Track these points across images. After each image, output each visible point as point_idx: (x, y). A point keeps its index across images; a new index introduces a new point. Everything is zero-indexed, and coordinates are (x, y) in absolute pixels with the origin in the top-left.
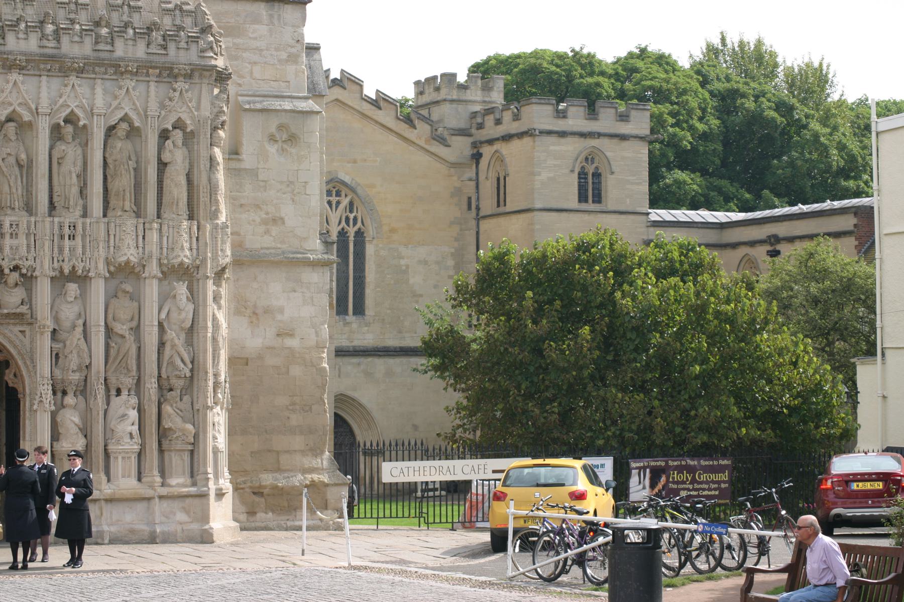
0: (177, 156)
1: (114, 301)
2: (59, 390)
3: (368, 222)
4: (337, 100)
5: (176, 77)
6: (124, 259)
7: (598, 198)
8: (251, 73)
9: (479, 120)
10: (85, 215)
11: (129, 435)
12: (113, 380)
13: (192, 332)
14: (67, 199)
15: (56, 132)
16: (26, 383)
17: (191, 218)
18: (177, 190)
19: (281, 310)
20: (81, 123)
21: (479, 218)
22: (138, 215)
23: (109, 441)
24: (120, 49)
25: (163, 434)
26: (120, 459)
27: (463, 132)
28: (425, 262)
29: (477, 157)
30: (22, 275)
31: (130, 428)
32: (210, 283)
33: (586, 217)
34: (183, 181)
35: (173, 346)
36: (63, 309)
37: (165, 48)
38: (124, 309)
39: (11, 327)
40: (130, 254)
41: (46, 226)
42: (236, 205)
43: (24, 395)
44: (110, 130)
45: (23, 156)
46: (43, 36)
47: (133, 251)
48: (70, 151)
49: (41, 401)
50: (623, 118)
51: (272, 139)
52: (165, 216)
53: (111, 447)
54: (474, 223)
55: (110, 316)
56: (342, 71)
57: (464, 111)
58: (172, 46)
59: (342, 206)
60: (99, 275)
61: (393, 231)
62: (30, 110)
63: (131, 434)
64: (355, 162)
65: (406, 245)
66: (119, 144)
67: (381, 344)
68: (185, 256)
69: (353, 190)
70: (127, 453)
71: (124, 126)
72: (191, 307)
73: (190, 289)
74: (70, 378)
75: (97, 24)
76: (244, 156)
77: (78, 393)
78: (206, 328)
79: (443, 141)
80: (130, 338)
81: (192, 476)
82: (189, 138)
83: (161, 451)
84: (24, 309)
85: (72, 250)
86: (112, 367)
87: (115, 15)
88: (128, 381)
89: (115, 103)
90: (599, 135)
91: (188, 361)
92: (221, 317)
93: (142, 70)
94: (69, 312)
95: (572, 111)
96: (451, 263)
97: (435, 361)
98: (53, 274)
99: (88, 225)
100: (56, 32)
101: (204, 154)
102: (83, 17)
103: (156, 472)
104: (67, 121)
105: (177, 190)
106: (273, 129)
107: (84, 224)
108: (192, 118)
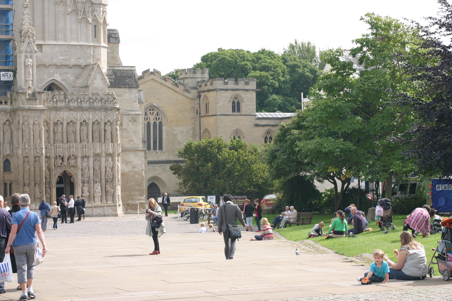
0: (108, 128)
1: (95, 162)
2: (83, 182)
3: (163, 119)
4: (152, 79)
5: (108, 110)
7: (239, 110)
8: (125, 105)
9: (200, 84)
10: (88, 143)
12: (95, 180)
13: (112, 168)
14: (84, 139)
15: (81, 123)
17: (112, 142)
18: (109, 136)
19: (133, 162)
21: (200, 117)
22: (100, 142)
24: (95, 105)
25: (106, 192)
27: (195, 88)
28: (183, 132)
29: (199, 96)
31: (99, 191)
32: (116, 157)
33: (235, 117)
34: (110, 134)
35: (108, 172)
37: (105, 103)
38: (97, 163)
40: (98, 151)
41: (80, 145)
42: (122, 137)
44: (93, 123)
45: (74, 130)
46: (78, 102)
47: (99, 150)
48: (84, 128)
50: (247, 84)
51: (130, 121)
52: (106, 142)
53: (95, 195)
54: (199, 118)
56: (154, 69)
57: (195, 81)
58: (107, 103)
59: (154, 114)
60: (91, 156)
61: (171, 122)
62: (75, 119)
64: (159, 99)
65: (176, 127)
66: (95, 126)
67: (168, 159)
68: (111, 151)
69: (158, 109)
71: (96, 122)
72: (112, 163)
73: (112, 158)
75: (90, 99)
76: (124, 126)
78: (116, 167)
79: (188, 91)
80: (99, 170)
81: (113, 201)
82: (111, 124)
83: (106, 196)
84: (75, 164)
85: (85, 151)
87: (94, 96)
88: (98, 180)
89: (94, 117)
90: (239, 90)
91: (112, 175)
92: (119, 165)
93: (100, 109)
94: (85, 165)
95: (230, 82)
96: (191, 132)
97: (174, 172)
100: (81, 101)
101: (114, 127)
102: (86, 97)
103: (105, 200)
104: (83, 121)
105: (109, 136)
106: (130, 119)
107: (88, 145)
108: (112, 119)
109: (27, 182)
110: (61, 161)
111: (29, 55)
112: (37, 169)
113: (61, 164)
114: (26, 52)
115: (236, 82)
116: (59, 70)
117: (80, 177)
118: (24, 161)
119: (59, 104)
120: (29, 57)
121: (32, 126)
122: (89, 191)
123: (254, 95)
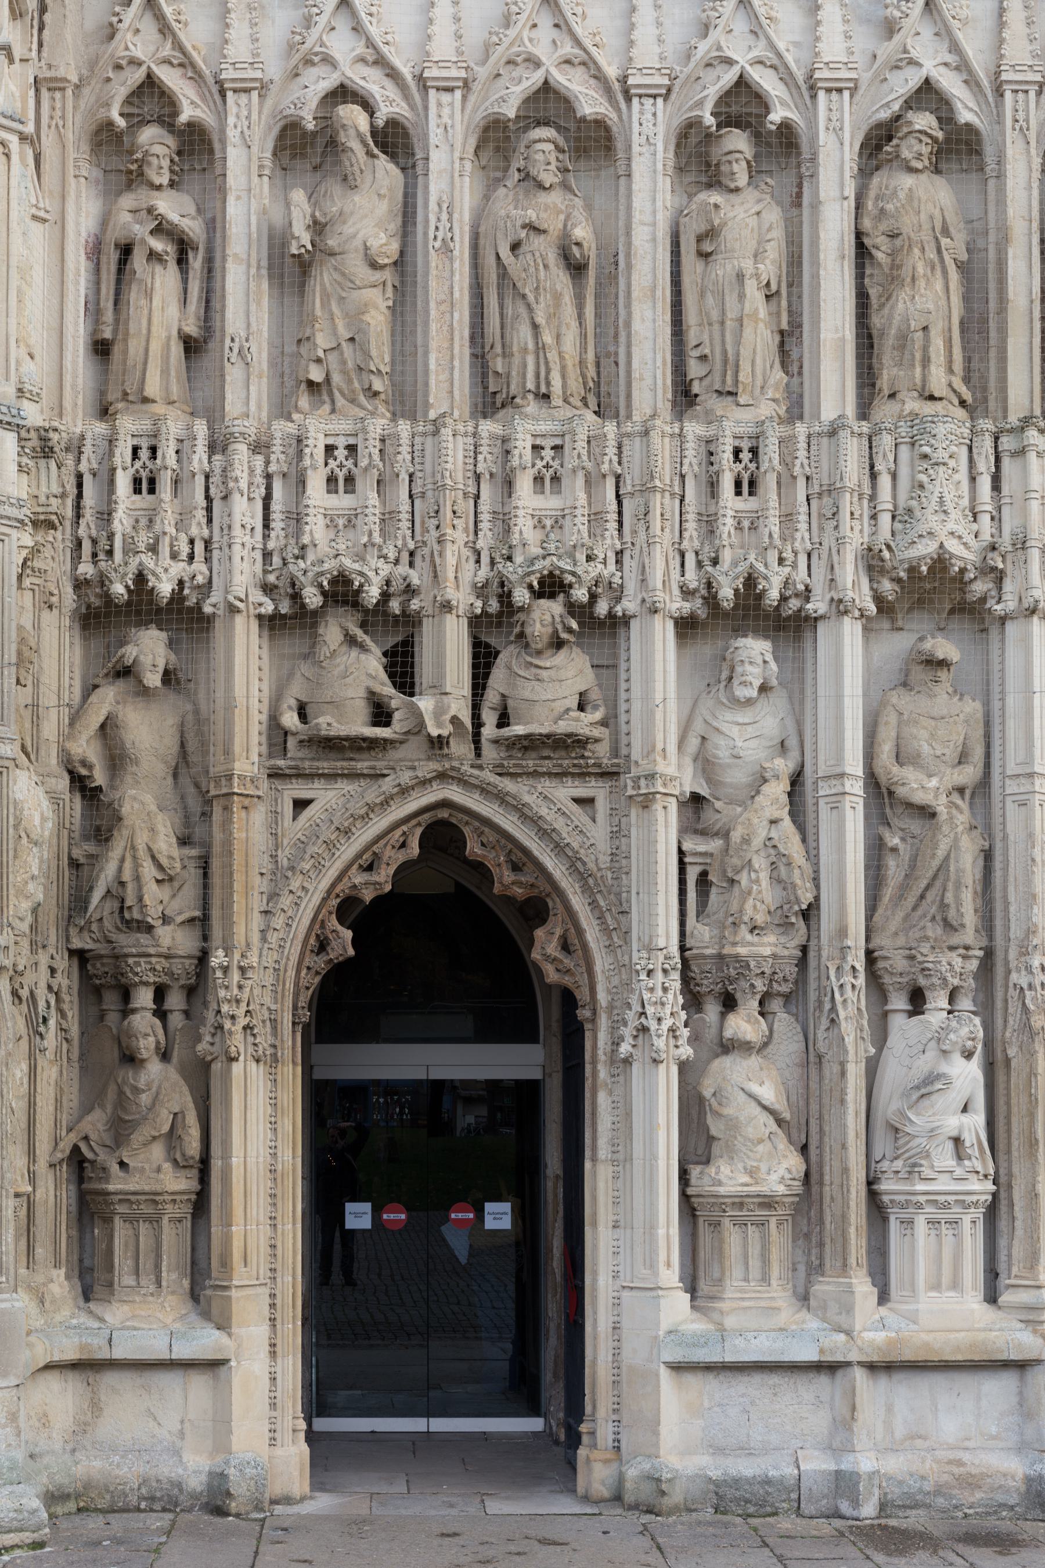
6: (926, 549)
11: (950, 1145)
12: (895, 961)
16: (598, 968)
20: (776, 116)
23: (885, 1165)
26: (920, 1222)
30: (573, 608)
31: (953, 1123)
36: (724, 727)
39: (545, 785)
43: (594, 1012)
45: (581, 232)
47: (957, 522)
49: (645, 1029)
55: (886, 751)
63: (957, 1141)
70: (946, 1206)
74: (742, 951)
77: (776, 1005)
84: (584, 724)
86: (891, 918)
89: (887, 50)
98: (686, 607)
99: (802, 445)
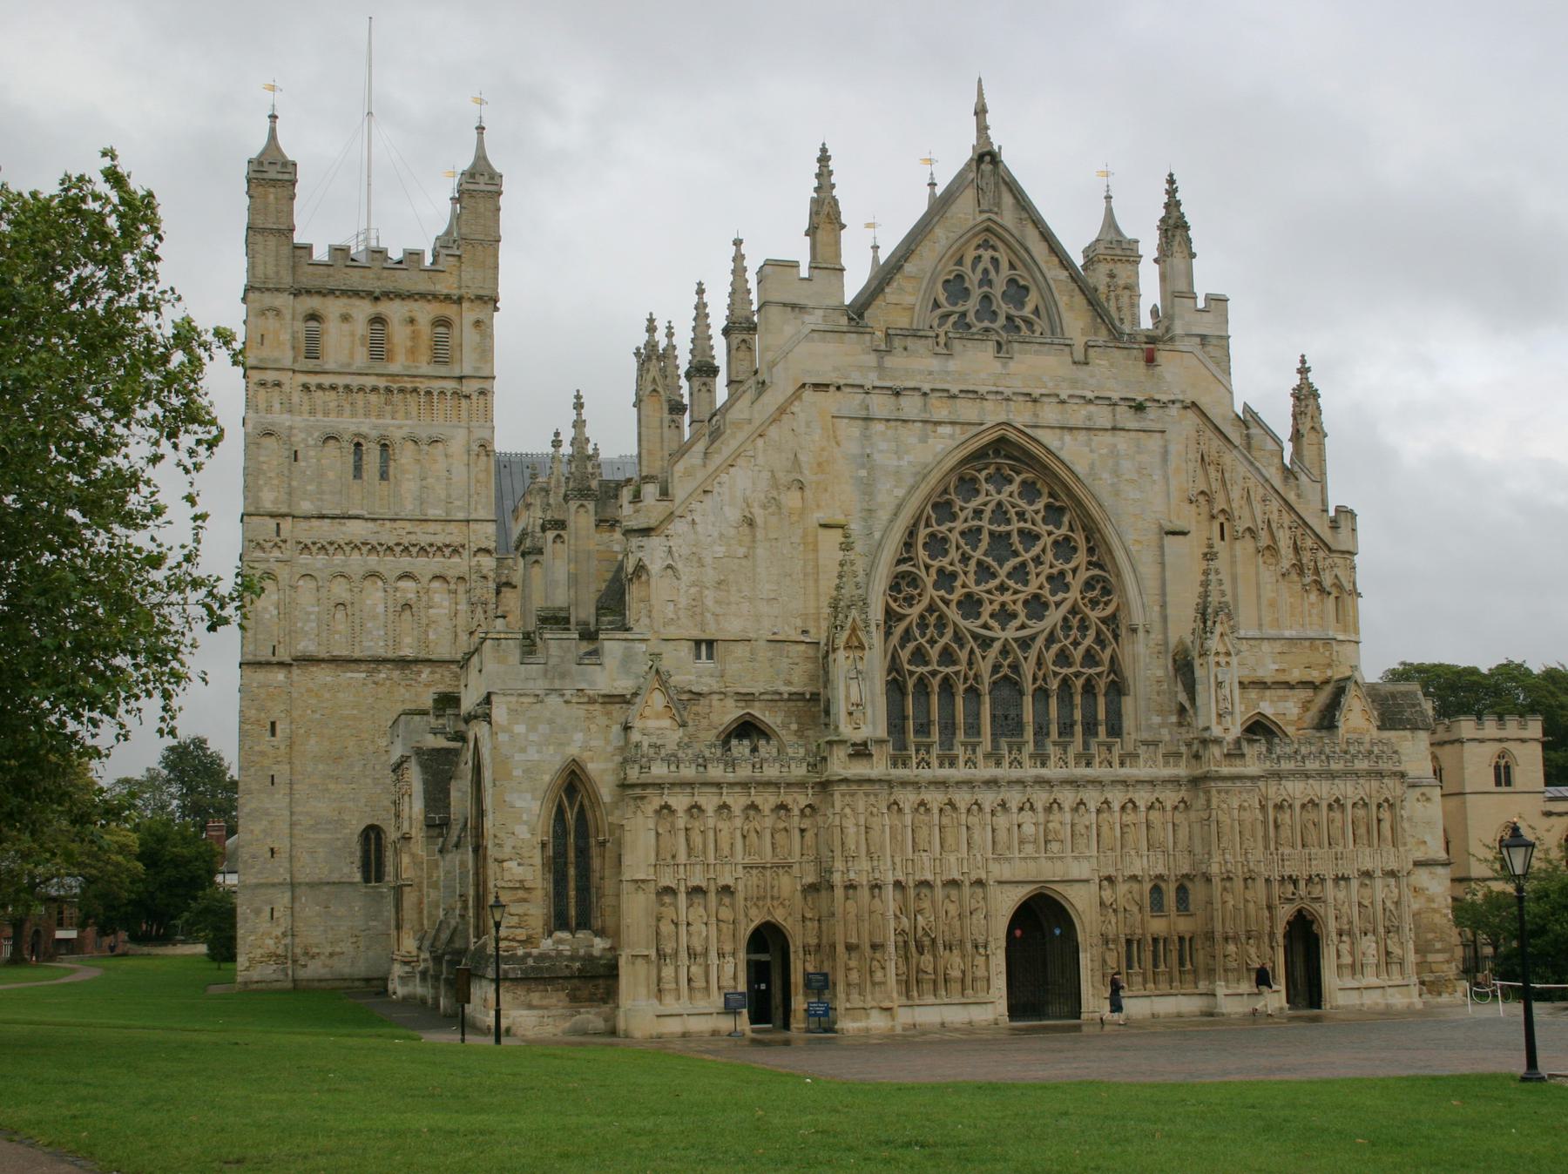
0: (1386, 815)
7: (1508, 783)
13: (1397, 903)
15: (1330, 806)
38: (1366, 892)
40: (1368, 866)
44: (1354, 805)
51: (1418, 800)
68: (1393, 866)
106: (1418, 795)
109: (1231, 934)
110: (1292, 887)
111: (1222, 660)
112: (1251, 906)
113: (1293, 894)
114: (1217, 654)
115: (1502, 726)
116: (1268, 693)
117: (1332, 926)
118: (1225, 889)
119: (1286, 765)
120: (1223, 663)
121: (1236, 812)
122: (1352, 953)
123: (1537, 750)
